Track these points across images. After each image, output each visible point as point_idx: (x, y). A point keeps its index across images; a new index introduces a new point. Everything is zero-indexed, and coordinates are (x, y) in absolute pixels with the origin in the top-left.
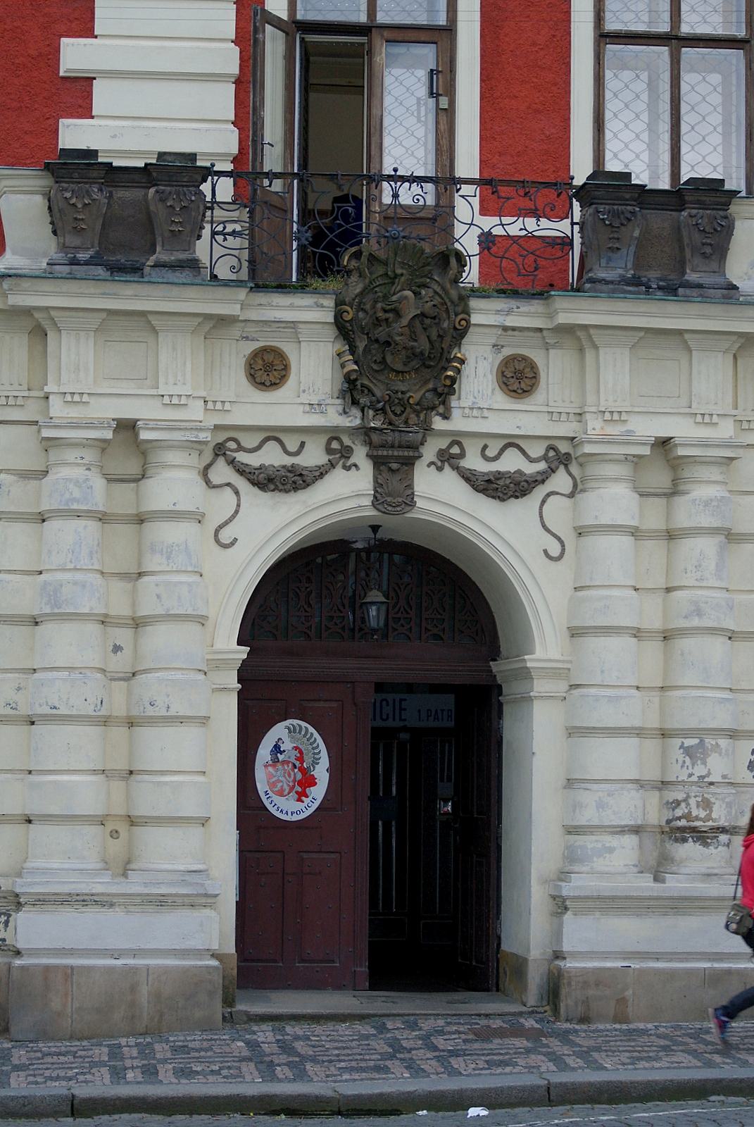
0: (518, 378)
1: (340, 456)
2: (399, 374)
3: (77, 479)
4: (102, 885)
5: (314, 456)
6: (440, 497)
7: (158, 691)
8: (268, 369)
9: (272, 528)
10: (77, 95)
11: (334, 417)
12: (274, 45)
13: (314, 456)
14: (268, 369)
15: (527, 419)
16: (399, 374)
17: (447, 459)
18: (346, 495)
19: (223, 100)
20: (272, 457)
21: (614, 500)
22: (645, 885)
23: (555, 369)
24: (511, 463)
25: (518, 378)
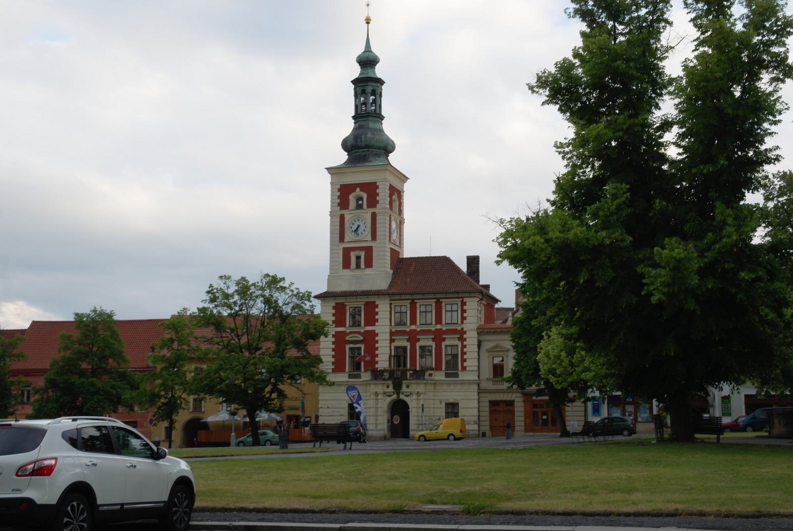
0: (408, 387)
1: (394, 394)
2: (397, 387)
3: (373, 396)
4: (375, 429)
5: (392, 394)
6: (402, 397)
7: (379, 413)
8: (388, 387)
9: (389, 399)
10: (377, 363)
11: (393, 390)
12: (392, 358)
13: (392, 394)
14: (388, 387)
15: (408, 390)
16: (397, 387)
17: (403, 393)
18: (395, 396)
19: (388, 362)
20: (389, 394)
21: (415, 397)
22: (417, 429)
23: (410, 386)
24: (408, 394)
25: (408, 387)
